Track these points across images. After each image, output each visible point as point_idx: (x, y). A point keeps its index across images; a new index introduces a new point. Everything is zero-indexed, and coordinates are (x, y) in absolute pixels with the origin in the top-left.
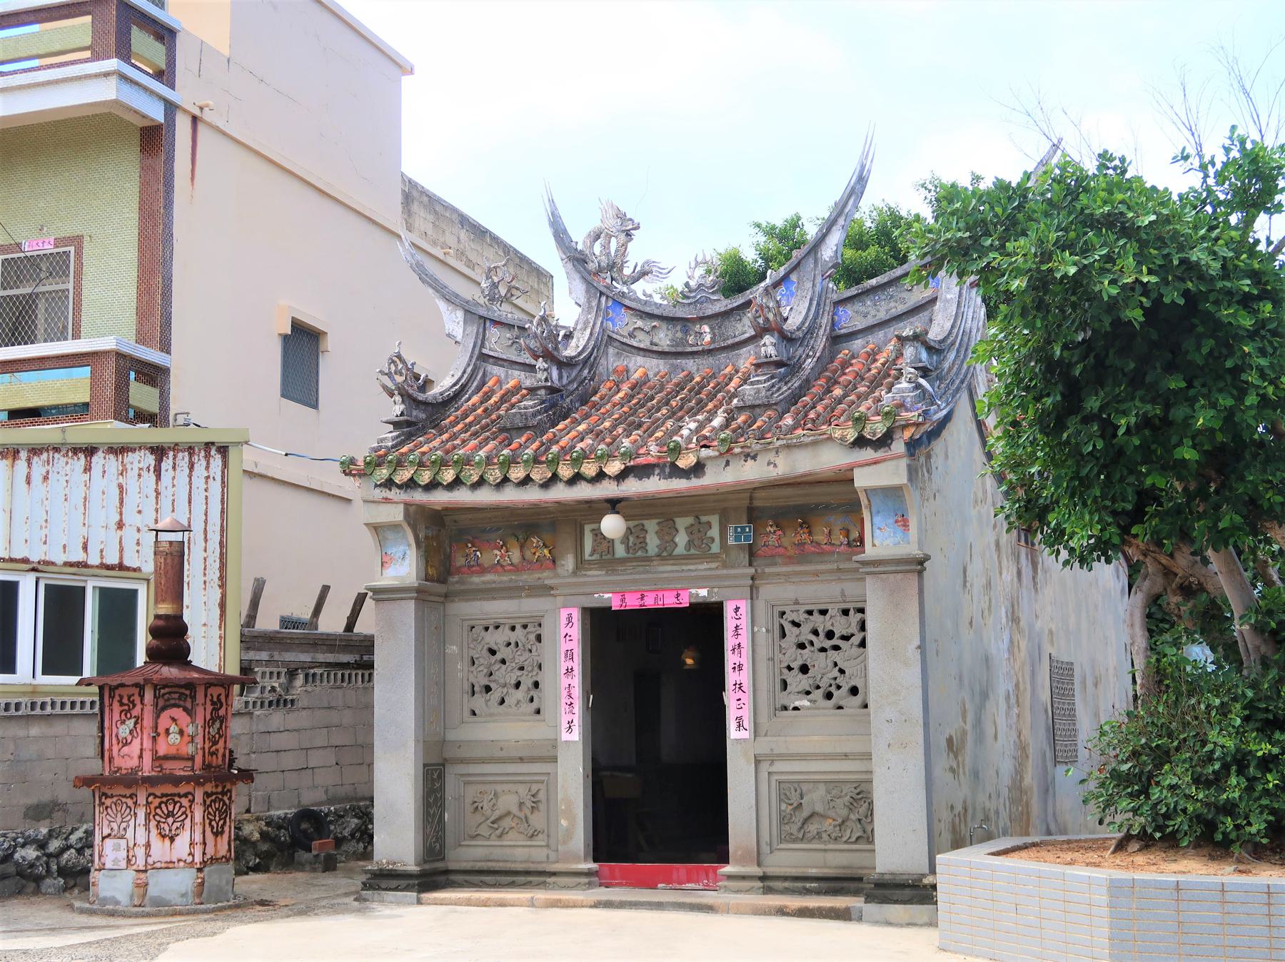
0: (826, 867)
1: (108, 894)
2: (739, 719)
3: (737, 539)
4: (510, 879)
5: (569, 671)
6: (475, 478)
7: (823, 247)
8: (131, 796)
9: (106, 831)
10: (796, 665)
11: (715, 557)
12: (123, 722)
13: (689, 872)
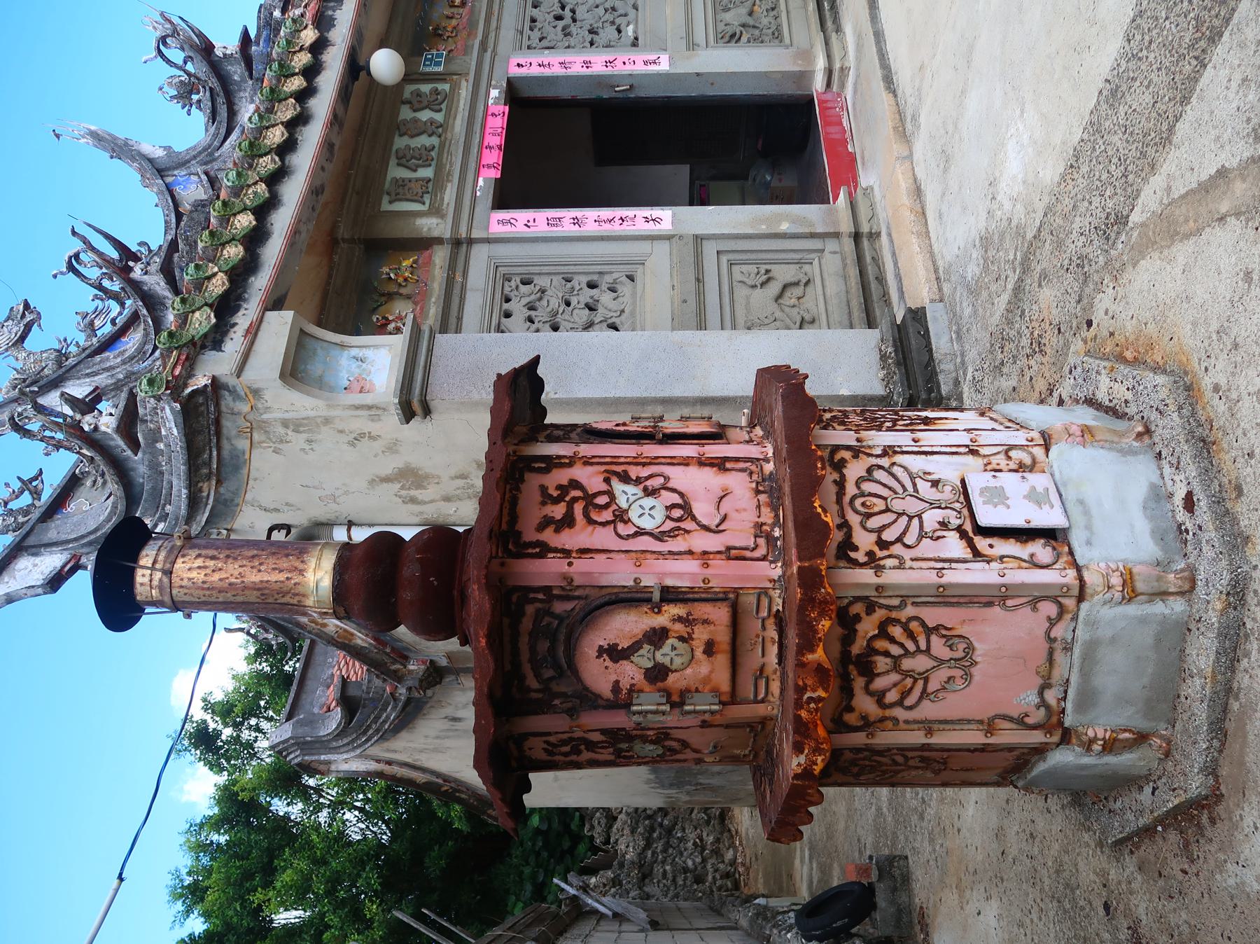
0: (805, 7)
1: (1142, 527)
2: (645, 63)
3: (438, 64)
4: (874, 285)
5: (576, 221)
6: (262, 188)
7: (152, 156)
8: (839, 466)
9: (954, 546)
10: (589, 37)
11: (455, 87)
12: (621, 516)
13: (827, 124)
